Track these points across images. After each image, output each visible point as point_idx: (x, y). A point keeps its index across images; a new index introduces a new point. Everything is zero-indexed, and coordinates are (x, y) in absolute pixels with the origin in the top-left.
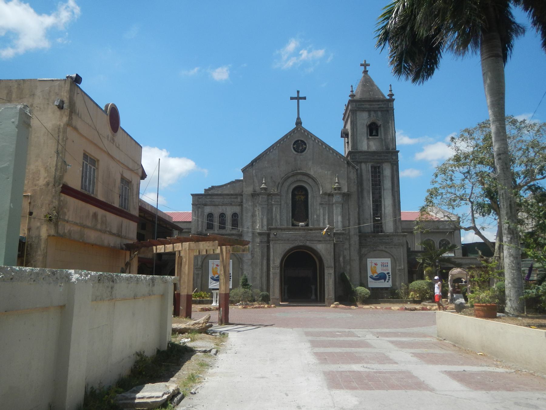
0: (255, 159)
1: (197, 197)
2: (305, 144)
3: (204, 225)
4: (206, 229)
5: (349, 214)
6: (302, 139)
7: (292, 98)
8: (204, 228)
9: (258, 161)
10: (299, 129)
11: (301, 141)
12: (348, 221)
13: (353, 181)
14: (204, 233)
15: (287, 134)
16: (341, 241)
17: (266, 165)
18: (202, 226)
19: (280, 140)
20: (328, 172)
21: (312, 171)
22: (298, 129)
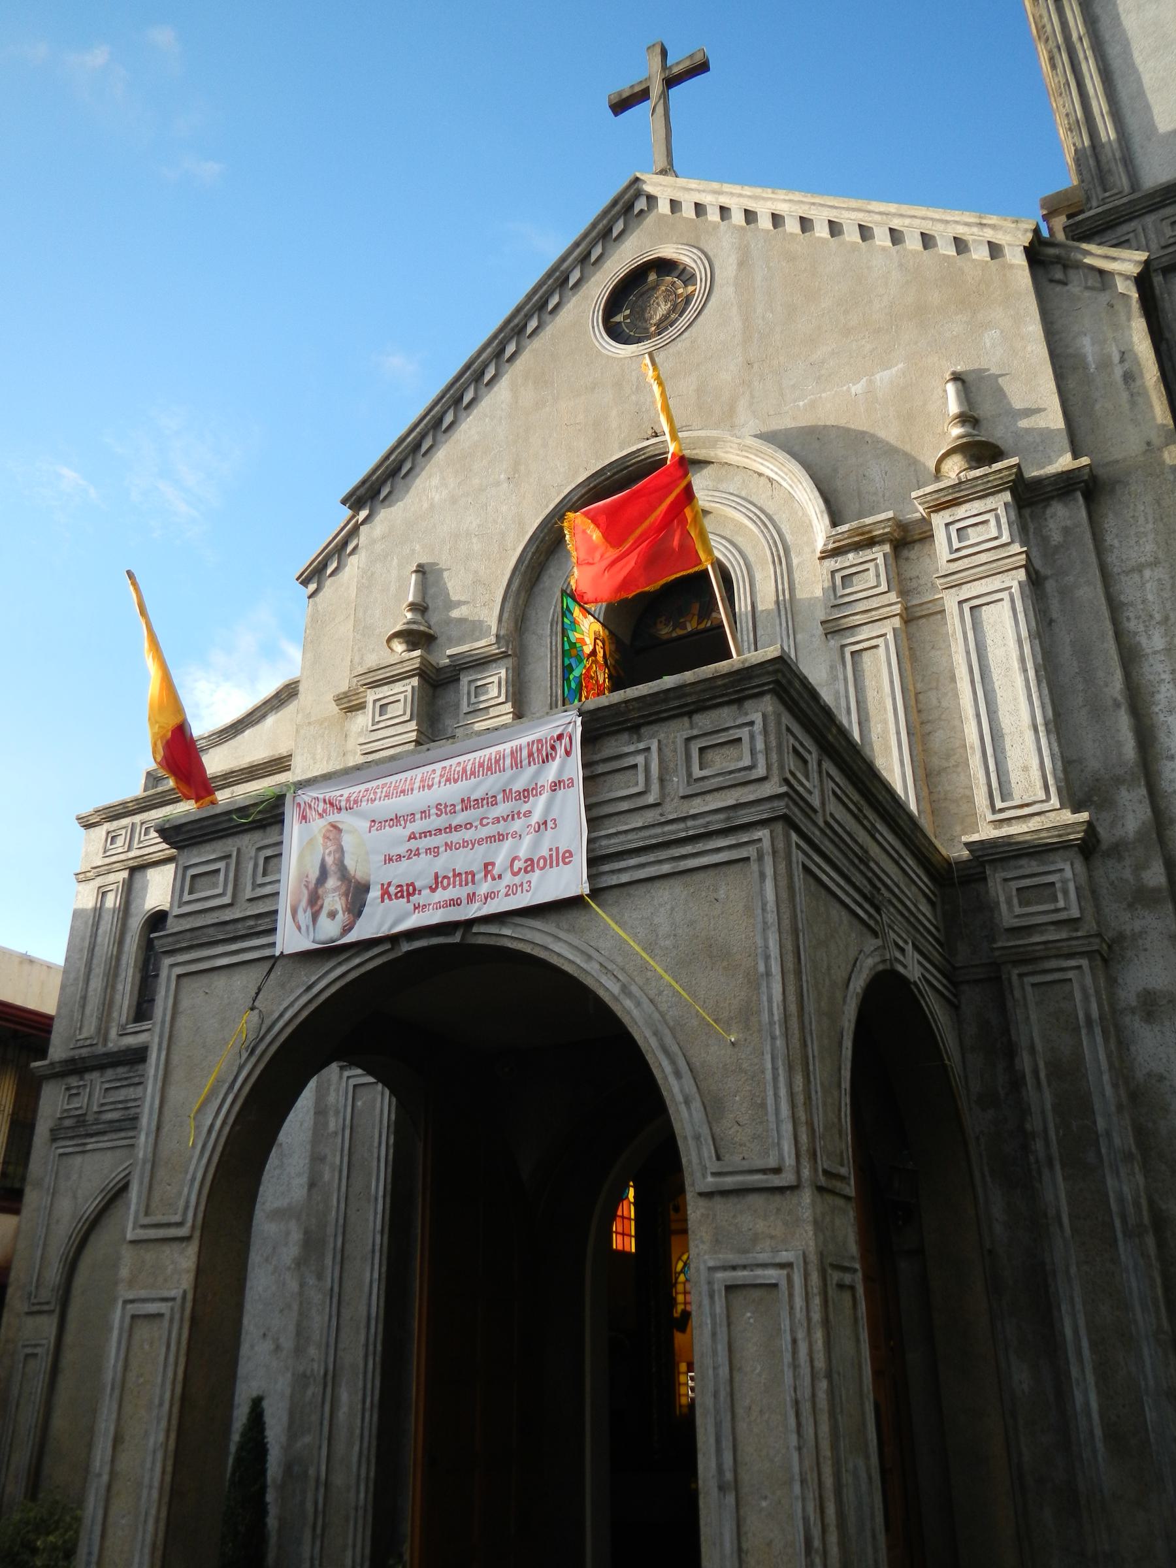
0: (364, 482)
1: (107, 826)
2: (688, 277)
3: (118, 997)
4: (124, 1019)
5: (1130, 656)
6: (668, 251)
7: (621, 106)
8: (115, 1015)
9: (384, 492)
10: (641, 204)
11: (664, 266)
12: (1123, 722)
13: (1118, 372)
14: (111, 1046)
15: (563, 259)
16: (1073, 923)
17: (437, 498)
18: (107, 1005)
19: (518, 310)
20: (870, 382)
21: (743, 414)
22: (630, 207)
